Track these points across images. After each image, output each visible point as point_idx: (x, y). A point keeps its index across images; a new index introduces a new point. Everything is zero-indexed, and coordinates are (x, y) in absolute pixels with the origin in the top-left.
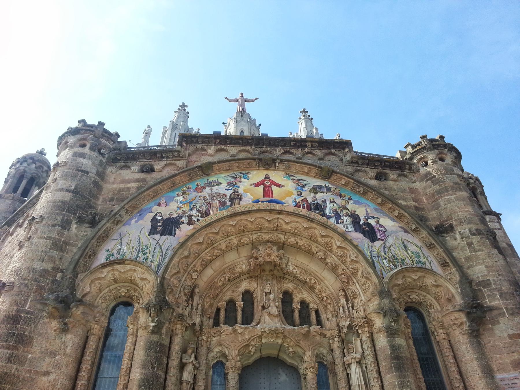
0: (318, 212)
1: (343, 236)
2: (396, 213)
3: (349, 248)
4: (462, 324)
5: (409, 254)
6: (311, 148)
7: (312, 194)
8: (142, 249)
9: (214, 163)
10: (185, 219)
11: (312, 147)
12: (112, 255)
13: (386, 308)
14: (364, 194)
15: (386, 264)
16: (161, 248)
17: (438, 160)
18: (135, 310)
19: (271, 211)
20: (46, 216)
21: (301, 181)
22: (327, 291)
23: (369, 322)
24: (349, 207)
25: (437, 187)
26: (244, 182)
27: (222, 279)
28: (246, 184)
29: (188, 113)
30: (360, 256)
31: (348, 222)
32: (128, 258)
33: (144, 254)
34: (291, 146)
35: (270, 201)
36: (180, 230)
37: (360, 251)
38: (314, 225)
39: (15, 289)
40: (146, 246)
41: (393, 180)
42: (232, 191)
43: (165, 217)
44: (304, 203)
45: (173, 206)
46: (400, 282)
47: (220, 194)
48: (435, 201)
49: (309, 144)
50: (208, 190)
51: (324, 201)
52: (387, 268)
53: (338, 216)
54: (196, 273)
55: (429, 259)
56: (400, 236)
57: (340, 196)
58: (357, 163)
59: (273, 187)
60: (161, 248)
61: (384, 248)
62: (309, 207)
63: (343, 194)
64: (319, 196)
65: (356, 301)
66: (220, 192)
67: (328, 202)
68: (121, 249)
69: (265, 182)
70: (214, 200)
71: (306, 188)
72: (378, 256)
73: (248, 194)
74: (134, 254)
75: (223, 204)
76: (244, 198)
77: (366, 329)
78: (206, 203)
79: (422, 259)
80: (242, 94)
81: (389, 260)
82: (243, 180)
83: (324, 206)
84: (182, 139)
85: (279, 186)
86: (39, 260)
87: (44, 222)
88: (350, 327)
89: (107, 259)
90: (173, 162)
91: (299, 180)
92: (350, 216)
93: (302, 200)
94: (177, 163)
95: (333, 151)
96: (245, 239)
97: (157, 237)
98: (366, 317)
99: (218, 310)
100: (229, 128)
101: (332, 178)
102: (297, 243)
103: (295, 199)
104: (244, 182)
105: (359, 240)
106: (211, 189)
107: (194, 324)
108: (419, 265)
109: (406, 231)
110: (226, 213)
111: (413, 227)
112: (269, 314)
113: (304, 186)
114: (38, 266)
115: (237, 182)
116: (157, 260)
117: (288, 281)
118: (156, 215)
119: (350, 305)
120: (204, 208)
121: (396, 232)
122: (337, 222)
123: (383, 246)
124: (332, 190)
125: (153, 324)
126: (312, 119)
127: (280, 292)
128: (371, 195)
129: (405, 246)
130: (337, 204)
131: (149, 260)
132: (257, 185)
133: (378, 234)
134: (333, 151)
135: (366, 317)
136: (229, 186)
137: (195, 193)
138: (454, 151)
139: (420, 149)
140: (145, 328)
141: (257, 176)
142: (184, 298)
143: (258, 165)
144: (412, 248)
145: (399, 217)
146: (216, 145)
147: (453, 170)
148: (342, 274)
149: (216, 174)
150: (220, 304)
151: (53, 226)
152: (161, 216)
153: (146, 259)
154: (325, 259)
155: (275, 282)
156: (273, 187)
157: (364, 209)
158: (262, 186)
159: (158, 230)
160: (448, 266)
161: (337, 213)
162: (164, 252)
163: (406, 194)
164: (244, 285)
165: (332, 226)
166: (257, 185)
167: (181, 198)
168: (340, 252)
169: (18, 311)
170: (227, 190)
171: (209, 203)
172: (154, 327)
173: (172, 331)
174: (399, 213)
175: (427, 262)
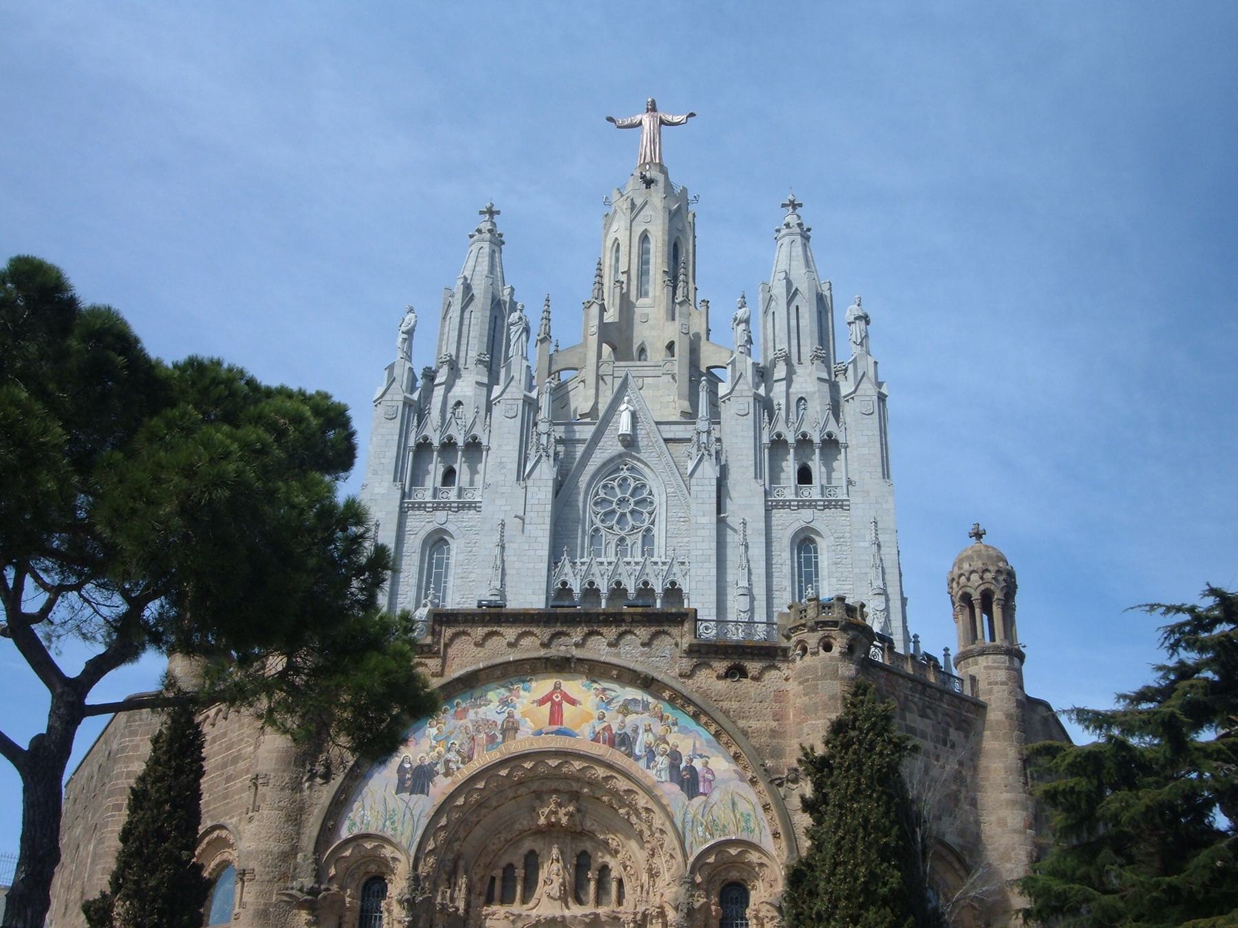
0: (623, 749)
1: (648, 791)
2: (733, 749)
3: (655, 808)
4: (772, 918)
5: (735, 817)
6: (631, 623)
7: (620, 716)
8: (389, 816)
9: (480, 670)
10: (440, 768)
11: (633, 621)
12: (354, 824)
13: (681, 900)
14: (695, 717)
15: (701, 834)
16: (411, 813)
17: (821, 648)
18: (388, 894)
19: (556, 754)
20: (273, 775)
21: (608, 692)
22: (633, 859)
23: (662, 914)
24: (671, 739)
25: (806, 699)
26: (524, 697)
27: (496, 841)
28: (525, 701)
29: (501, 235)
30: (668, 823)
31: (663, 766)
32: (372, 830)
33: (393, 823)
34: (599, 622)
35: (558, 732)
36: (435, 786)
37: (670, 817)
38: (614, 774)
39: (257, 877)
40: (394, 811)
41: (755, 679)
42: (506, 715)
43: (415, 765)
44: (606, 734)
45: (425, 744)
46: (711, 860)
47: (488, 721)
48: (799, 724)
49: (628, 619)
50: (471, 714)
51: (636, 730)
52: (702, 839)
53: (651, 754)
54: (458, 842)
55: (762, 824)
56: (732, 787)
57: (662, 718)
58: (699, 651)
59: (565, 705)
60: (411, 813)
61: (704, 808)
62: (611, 742)
63: (665, 714)
64: (631, 718)
65: (657, 880)
66: (488, 718)
67: (641, 731)
68: (364, 815)
69: (554, 697)
70: (479, 732)
71: (613, 705)
72: (693, 821)
73: (528, 719)
74: (381, 824)
75: (492, 739)
76: (521, 728)
77: (660, 920)
78: (469, 738)
79: (752, 824)
80: (653, 102)
81: (706, 827)
82: (522, 693)
83: (634, 738)
84: (435, 621)
85: (573, 702)
86: (275, 840)
87: (271, 786)
88: (644, 915)
89: (350, 830)
90: (423, 660)
91: (604, 690)
92: (668, 755)
93: (604, 729)
94: (428, 661)
95: (666, 628)
96: (523, 790)
97: (406, 796)
98: (661, 907)
99: (493, 879)
100: (615, 227)
101: (652, 687)
102: (594, 793)
103: (594, 728)
104: (524, 697)
105: (673, 796)
106: (476, 713)
107: (457, 909)
108: (744, 836)
109: (742, 779)
110: (494, 756)
111: (749, 775)
112: (549, 896)
113: (609, 703)
114: (275, 847)
115: (514, 698)
116: (408, 833)
117: (586, 838)
118: (403, 762)
119: (651, 883)
120: (466, 747)
121: (729, 780)
122: (648, 767)
123: (703, 806)
124: (651, 706)
125: (407, 919)
126: (809, 230)
127: (573, 854)
128: (704, 719)
129: (734, 804)
130: (654, 734)
131: (399, 832)
132: (541, 702)
133: (701, 784)
134: (666, 628)
135: (661, 907)
136: (501, 707)
137: (453, 721)
138: (852, 629)
139: (799, 626)
140: (399, 922)
141: (543, 686)
142: (445, 877)
143: (544, 666)
144: (743, 807)
145: (736, 757)
146: (485, 624)
147: (837, 670)
148: (648, 842)
149: (483, 685)
150: (495, 872)
151: (282, 789)
152: (410, 763)
153: (395, 829)
154: (629, 817)
155: (568, 840)
156: (565, 705)
157: (692, 742)
158: (549, 704)
159: (406, 785)
160: (779, 838)
161: (652, 751)
162: (416, 819)
163: (766, 705)
164: (527, 845)
165: (638, 775)
166: (541, 702)
167: (434, 731)
168: (644, 815)
169: (266, 904)
170: (499, 713)
171: (473, 739)
172: (408, 922)
173: (432, 920)
174: (735, 753)
175: (757, 829)
